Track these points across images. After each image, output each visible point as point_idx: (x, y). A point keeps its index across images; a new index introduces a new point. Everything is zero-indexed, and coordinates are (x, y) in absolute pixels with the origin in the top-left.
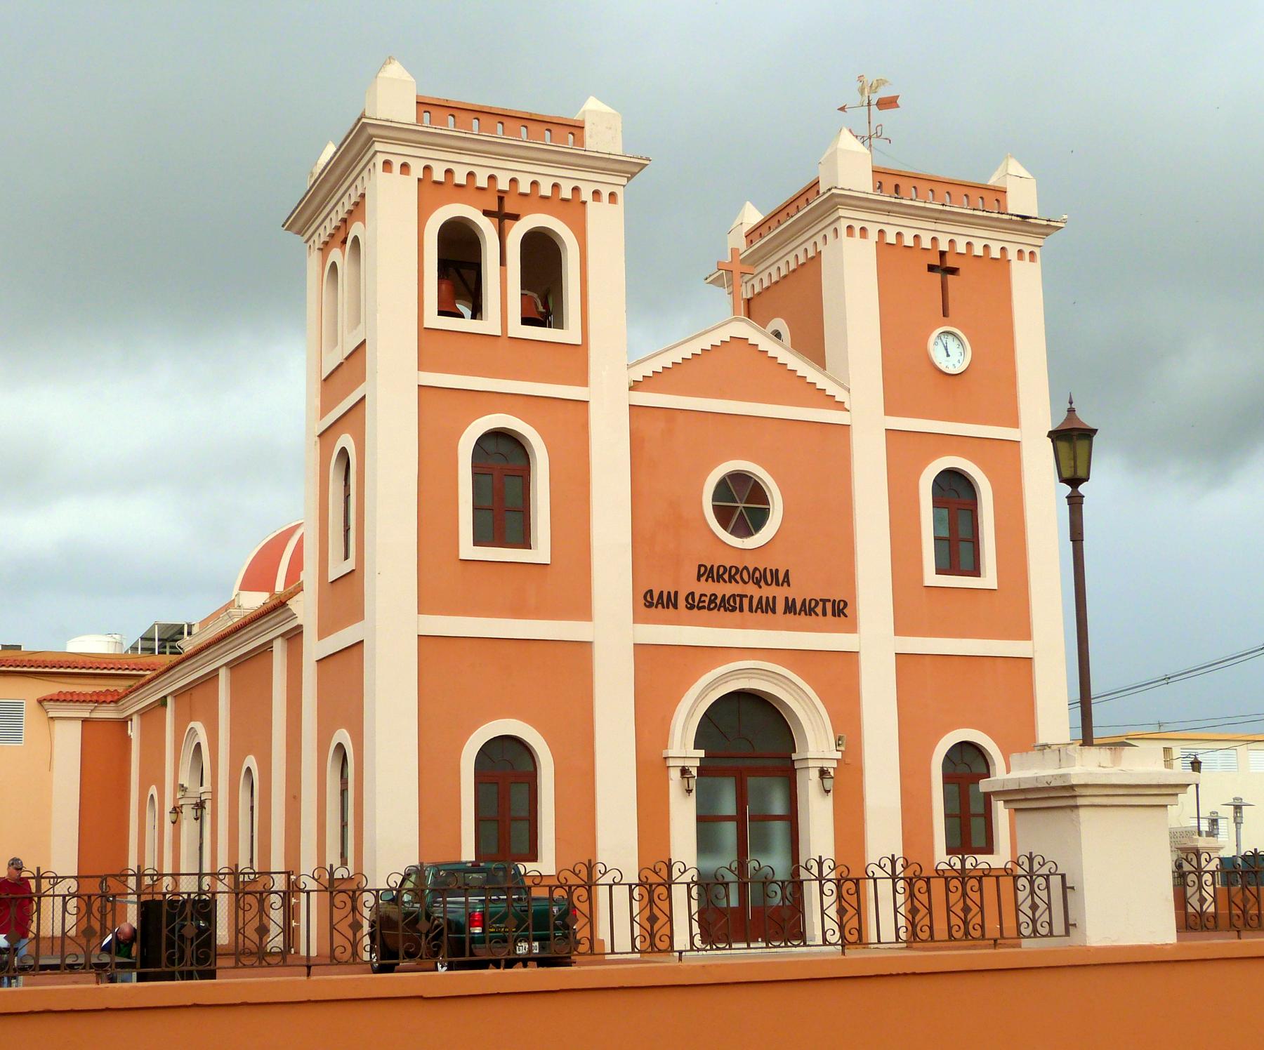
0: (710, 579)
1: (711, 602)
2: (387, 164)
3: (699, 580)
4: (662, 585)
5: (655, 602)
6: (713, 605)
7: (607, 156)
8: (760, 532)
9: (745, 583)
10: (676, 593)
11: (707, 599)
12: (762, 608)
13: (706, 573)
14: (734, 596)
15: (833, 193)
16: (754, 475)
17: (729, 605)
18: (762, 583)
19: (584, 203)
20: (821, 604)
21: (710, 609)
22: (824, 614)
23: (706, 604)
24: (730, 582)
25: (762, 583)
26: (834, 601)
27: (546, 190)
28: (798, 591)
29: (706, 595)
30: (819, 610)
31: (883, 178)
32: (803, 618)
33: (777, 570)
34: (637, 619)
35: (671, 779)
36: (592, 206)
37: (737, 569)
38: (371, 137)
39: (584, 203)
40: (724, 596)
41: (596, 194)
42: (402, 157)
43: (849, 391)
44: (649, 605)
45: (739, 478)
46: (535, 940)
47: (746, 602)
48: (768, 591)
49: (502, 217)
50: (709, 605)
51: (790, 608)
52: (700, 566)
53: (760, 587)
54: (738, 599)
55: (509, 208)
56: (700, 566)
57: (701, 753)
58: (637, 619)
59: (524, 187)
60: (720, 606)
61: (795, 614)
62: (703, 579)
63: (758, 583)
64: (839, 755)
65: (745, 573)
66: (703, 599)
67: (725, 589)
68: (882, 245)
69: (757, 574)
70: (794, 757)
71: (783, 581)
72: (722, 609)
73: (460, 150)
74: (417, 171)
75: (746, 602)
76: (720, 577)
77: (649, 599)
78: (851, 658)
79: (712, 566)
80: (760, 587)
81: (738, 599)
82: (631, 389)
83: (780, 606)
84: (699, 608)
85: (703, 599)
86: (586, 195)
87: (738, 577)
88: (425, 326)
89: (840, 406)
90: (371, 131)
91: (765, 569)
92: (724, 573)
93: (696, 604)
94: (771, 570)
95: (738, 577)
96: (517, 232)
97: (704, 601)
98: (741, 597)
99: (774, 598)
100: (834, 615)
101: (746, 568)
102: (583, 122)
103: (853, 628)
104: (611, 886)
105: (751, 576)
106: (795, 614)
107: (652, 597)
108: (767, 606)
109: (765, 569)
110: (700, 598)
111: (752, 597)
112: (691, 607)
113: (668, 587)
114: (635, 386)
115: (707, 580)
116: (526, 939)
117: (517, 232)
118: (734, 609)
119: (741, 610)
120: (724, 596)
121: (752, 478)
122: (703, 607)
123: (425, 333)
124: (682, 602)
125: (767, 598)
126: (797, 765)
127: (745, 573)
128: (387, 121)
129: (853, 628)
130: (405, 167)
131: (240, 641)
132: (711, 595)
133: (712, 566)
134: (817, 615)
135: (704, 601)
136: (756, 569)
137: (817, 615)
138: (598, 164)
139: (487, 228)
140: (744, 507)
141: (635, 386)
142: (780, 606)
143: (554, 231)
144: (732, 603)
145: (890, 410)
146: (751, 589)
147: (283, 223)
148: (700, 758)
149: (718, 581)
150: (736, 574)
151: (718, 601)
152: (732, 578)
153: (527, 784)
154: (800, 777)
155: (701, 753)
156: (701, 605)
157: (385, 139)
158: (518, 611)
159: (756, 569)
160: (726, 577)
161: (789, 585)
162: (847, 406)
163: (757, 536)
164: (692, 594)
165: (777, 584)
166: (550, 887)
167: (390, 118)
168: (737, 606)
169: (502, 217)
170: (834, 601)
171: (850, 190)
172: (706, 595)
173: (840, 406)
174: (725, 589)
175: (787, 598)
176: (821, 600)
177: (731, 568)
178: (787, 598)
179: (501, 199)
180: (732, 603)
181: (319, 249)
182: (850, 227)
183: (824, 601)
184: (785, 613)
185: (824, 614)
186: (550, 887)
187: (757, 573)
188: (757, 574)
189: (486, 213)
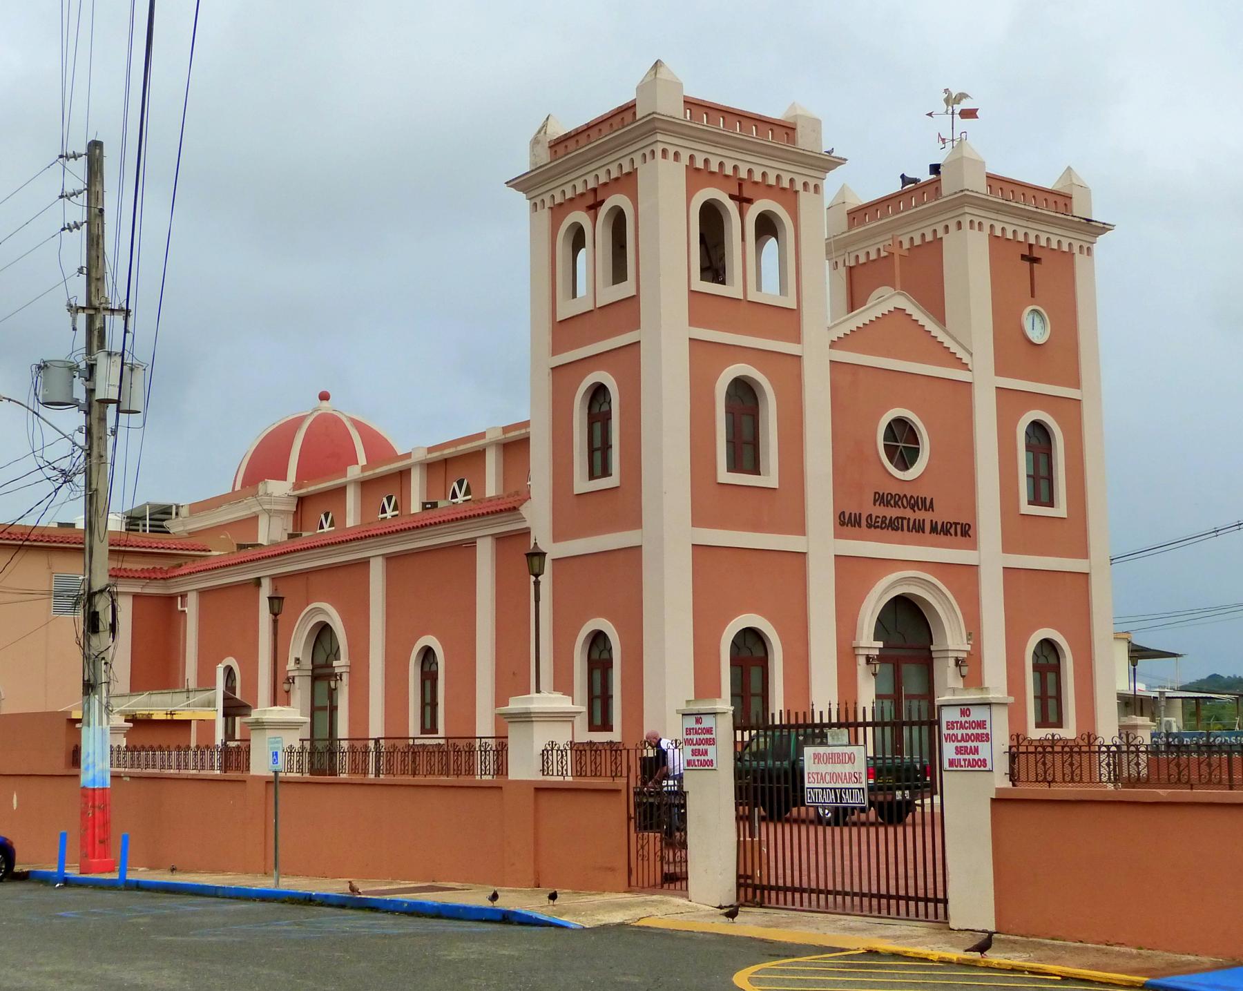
0: (882, 504)
1: (883, 522)
2: (664, 152)
3: (875, 505)
4: (851, 509)
5: (846, 521)
6: (884, 525)
7: (802, 152)
8: (914, 467)
9: (905, 508)
10: (860, 514)
11: (880, 520)
12: (915, 529)
13: (880, 499)
14: (897, 518)
15: (965, 194)
16: (911, 421)
17: (893, 525)
18: (916, 508)
19: (797, 192)
20: (954, 526)
21: (882, 528)
22: (956, 535)
23: (879, 524)
24: (895, 507)
25: (916, 508)
26: (962, 524)
27: (714, 167)
28: (940, 515)
29: (879, 517)
30: (952, 531)
31: (993, 182)
32: (942, 537)
33: (925, 498)
34: (837, 536)
35: (859, 665)
36: (802, 194)
37: (899, 496)
38: (656, 128)
39: (797, 192)
40: (891, 517)
41: (805, 184)
42: (777, 170)
43: (971, 355)
44: (842, 524)
45: (900, 422)
46: (906, 789)
47: (905, 522)
48: (920, 515)
49: (742, 201)
50: (882, 524)
51: (934, 529)
52: (875, 493)
53: (914, 511)
54: (900, 520)
55: (746, 194)
56: (875, 493)
57: (880, 644)
58: (837, 536)
59: (757, 177)
60: (888, 527)
61: (937, 534)
62: (878, 503)
63: (912, 508)
64: (968, 648)
65: (905, 499)
66: (878, 520)
67: (892, 513)
68: (993, 238)
69: (912, 501)
70: (932, 648)
71: (929, 507)
72: (890, 528)
73: (716, 144)
74: (685, 160)
75: (905, 522)
76: (888, 503)
77: (842, 519)
78: (973, 569)
79: (883, 494)
80: (914, 511)
81: (900, 520)
82: (831, 347)
83: (928, 527)
84: (875, 527)
85: (878, 520)
86: (799, 186)
87: (900, 503)
88: (692, 289)
89: (965, 366)
90: (658, 124)
91: (918, 497)
92: (891, 499)
93: (873, 523)
94: (922, 498)
95: (900, 503)
96: (753, 212)
97: (878, 522)
98: (903, 518)
99: (924, 520)
100: (962, 535)
101: (905, 496)
102: (796, 124)
103: (974, 546)
104: (1027, 746)
105: (909, 503)
106: (937, 534)
107: (844, 517)
108: (918, 527)
109: (918, 497)
110: (876, 519)
111: (909, 519)
112: (869, 526)
113: (855, 510)
114: (833, 345)
115: (880, 505)
116: (899, 788)
117: (753, 212)
118: (897, 529)
119: (902, 530)
120: (891, 517)
121: (907, 423)
122: (878, 527)
123: (693, 293)
124: (864, 522)
125: (919, 520)
126: (934, 655)
127: (905, 499)
128: (671, 117)
129: (974, 546)
130: (677, 156)
131: (436, 532)
132: (883, 517)
133: (883, 494)
134: (951, 535)
135: (878, 522)
136: (912, 497)
137: (951, 535)
138: (769, 151)
139: (731, 206)
140: (903, 447)
141: (833, 345)
142: (928, 527)
143: (724, 205)
144: (896, 524)
145: (999, 372)
146: (908, 513)
147: (508, 180)
148: (880, 648)
149: (887, 506)
150: (898, 500)
151: (887, 522)
152: (896, 504)
153: (740, 668)
154: (937, 665)
155: (880, 644)
156: (876, 524)
157: (666, 132)
158: (757, 527)
159: (912, 497)
160: (892, 502)
161: (933, 510)
162: (970, 367)
163: (911, 470)
164: (871, 515)
165: (926, 510)
166: (1035, 746)
167: (673, 115)
168: (900, 526)
169: (742, 201)
170: (962, 524)
171: (977, 192)
172: (879, 517)
173: (965, 366)
174: (892, 513)
175: (932, 521)
176: (954, 523)
177: (895, 495)
178: (932, 521)
179: (740, 185)
180: (896, 524)
181: (549, 208)
182: (971, 222)
183: (956, 524)
184: (930, 533)
185: (956, 535)
186: (1035, 746)
187: (913, 500)
188: (912, 501)
189: (732, 197)
